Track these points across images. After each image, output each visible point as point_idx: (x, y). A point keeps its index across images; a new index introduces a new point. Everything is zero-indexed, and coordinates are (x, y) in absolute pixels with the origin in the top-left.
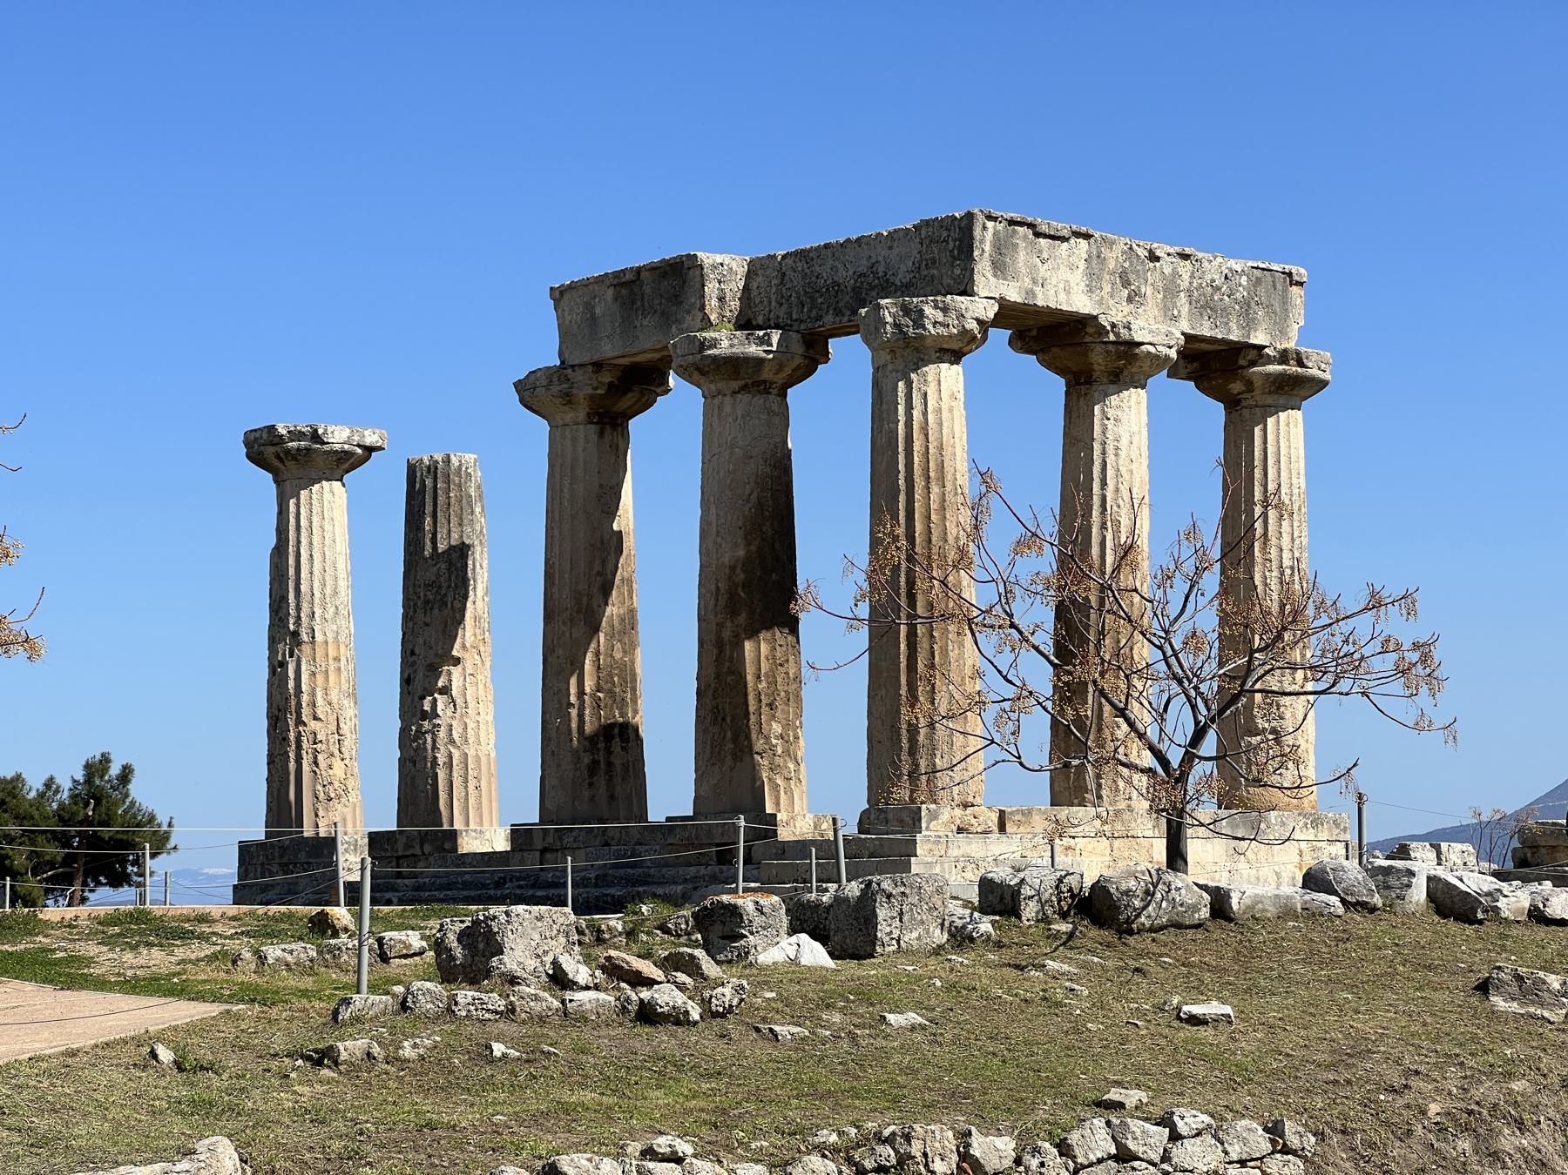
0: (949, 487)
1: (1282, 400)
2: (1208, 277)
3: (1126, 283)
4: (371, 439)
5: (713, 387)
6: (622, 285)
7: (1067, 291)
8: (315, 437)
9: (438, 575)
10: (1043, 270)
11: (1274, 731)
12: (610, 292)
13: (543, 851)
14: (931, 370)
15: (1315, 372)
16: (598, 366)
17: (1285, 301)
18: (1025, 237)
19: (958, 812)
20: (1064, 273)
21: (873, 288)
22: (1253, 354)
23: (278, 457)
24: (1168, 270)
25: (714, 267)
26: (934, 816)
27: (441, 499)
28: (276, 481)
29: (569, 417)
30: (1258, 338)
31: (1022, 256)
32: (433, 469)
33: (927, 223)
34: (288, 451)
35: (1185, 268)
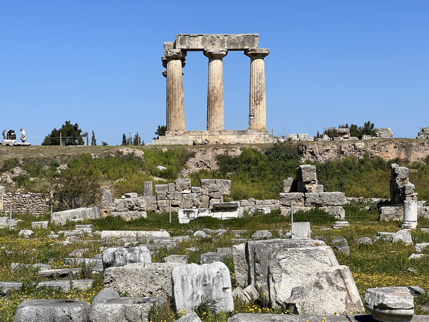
0: (174, 80)
1: (256, 57)
2: (232, 38)
3: (211, 42)
7: (197, 45)
10: (192, 42)
11: (253, 116)
14: (171, 62)
15: (259, 52)
17: (253, 41)
18: (187, 38)
19: (175, 132)
20: (196, 42)
22: (247, 50)
24: (221, 39)
25: (166, 45)
26: (168, 133)
30: (246, 47)
31: (187, 41)
35: (226, 38)
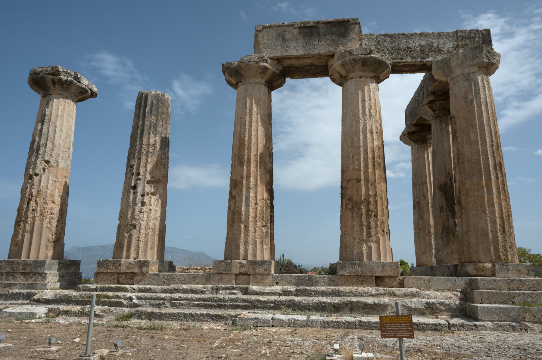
4: (95, 89)
5: (361, 74)
6: (305, 27)
8: (76, 78)
9: (155, 142)
12: (296, 31)
13: (236, 275)
16: (278, 60)
21: (432, 51)
23: (54, 82)
27: (160, 110)
28: (44, 96)
29: (259, 80)
32: (157, 97)
33: (462, 31)
34: (60, 80)
